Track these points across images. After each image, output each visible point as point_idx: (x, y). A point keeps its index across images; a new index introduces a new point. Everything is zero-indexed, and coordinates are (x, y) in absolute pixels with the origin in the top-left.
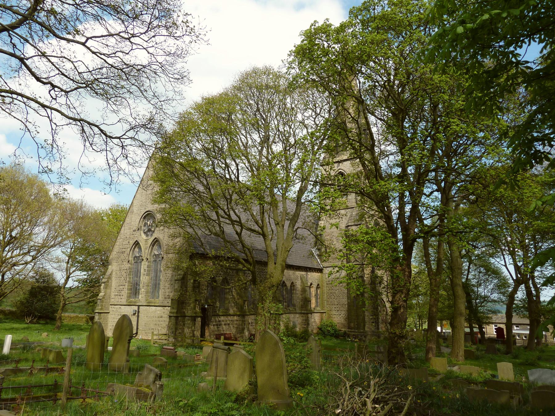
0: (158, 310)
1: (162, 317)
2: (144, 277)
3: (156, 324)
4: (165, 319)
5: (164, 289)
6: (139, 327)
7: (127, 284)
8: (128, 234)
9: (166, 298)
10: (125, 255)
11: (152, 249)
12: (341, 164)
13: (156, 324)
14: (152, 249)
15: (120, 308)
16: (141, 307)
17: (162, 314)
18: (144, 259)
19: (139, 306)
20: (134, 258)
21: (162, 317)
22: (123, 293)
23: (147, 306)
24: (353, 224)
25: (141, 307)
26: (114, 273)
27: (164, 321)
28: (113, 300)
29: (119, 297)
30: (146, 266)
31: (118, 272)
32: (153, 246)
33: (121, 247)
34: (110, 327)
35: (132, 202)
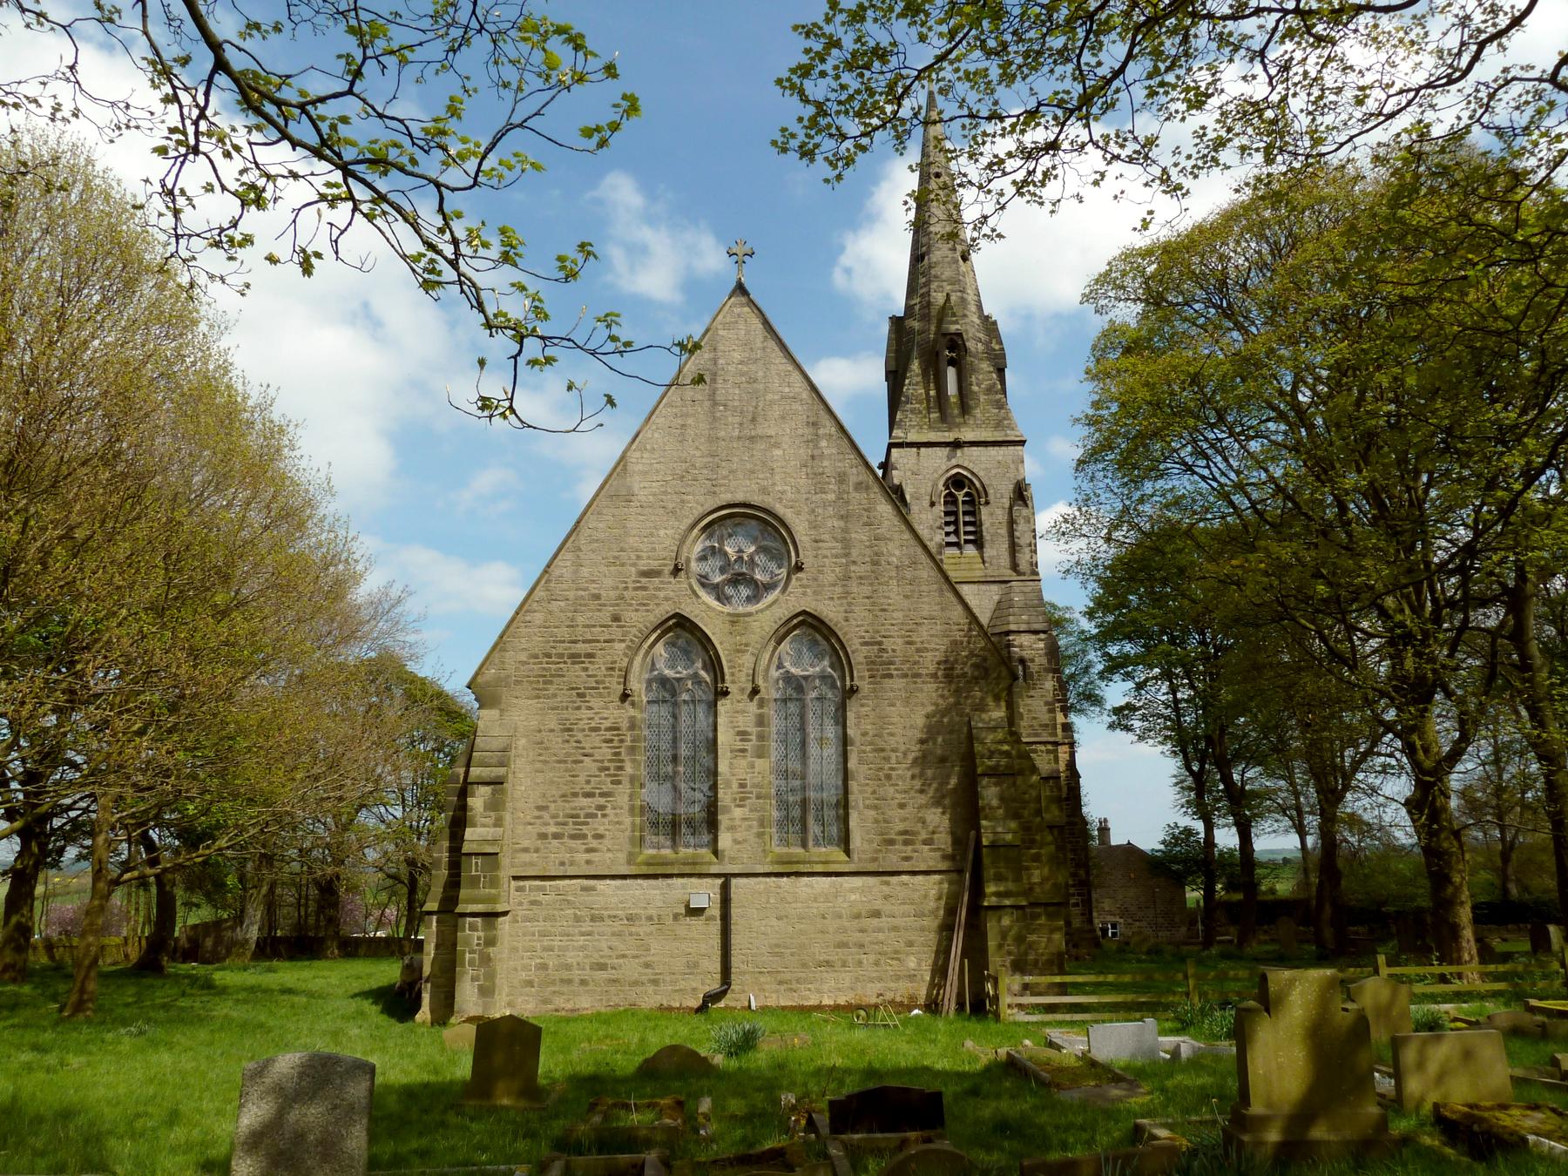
0: (852, 890)
1: (876, 914)
2: (743, 763)
3: (842, 945)
4: (899, 922)
5: (876, 807)
6: (736, 961)
7: (624, 790)
8: (609, 582)
9: (891, 842)
10: (598, 668)
11: (775, 649)
12: (959, 453)
13: (842, 945)
14: (775, 649)
15: (584, 889)
16: (734, 881)
17: (878, 904)
18: (732, 688)
19: (727, 877)
20: (649, 682)
21: (876, 914)
22: (599, 825)
23: (788, 875)
24: (1023, 627)
25: (734, 881)
26: (523, 742)
27: (895, 929)
28: (526, 857)
29: (577, 844)
30: (747, 722)
31: (556, 741)
32: (779, 643)
33: (563, 633)
34: (524, 975)
35: (623, 457)
